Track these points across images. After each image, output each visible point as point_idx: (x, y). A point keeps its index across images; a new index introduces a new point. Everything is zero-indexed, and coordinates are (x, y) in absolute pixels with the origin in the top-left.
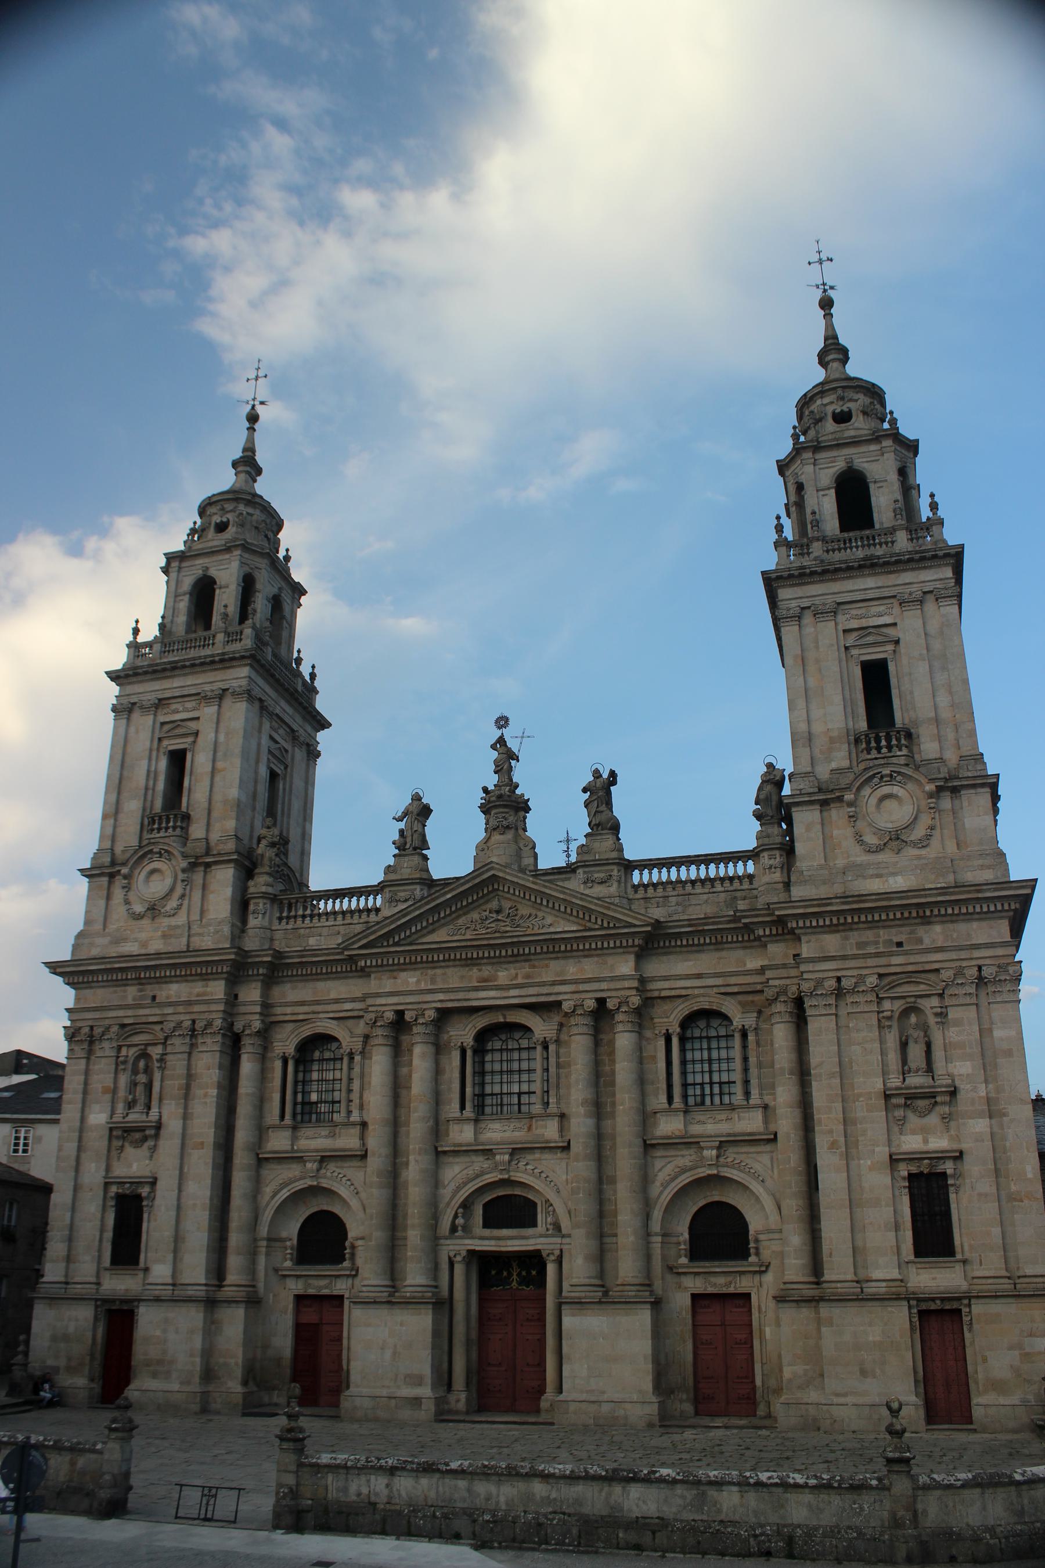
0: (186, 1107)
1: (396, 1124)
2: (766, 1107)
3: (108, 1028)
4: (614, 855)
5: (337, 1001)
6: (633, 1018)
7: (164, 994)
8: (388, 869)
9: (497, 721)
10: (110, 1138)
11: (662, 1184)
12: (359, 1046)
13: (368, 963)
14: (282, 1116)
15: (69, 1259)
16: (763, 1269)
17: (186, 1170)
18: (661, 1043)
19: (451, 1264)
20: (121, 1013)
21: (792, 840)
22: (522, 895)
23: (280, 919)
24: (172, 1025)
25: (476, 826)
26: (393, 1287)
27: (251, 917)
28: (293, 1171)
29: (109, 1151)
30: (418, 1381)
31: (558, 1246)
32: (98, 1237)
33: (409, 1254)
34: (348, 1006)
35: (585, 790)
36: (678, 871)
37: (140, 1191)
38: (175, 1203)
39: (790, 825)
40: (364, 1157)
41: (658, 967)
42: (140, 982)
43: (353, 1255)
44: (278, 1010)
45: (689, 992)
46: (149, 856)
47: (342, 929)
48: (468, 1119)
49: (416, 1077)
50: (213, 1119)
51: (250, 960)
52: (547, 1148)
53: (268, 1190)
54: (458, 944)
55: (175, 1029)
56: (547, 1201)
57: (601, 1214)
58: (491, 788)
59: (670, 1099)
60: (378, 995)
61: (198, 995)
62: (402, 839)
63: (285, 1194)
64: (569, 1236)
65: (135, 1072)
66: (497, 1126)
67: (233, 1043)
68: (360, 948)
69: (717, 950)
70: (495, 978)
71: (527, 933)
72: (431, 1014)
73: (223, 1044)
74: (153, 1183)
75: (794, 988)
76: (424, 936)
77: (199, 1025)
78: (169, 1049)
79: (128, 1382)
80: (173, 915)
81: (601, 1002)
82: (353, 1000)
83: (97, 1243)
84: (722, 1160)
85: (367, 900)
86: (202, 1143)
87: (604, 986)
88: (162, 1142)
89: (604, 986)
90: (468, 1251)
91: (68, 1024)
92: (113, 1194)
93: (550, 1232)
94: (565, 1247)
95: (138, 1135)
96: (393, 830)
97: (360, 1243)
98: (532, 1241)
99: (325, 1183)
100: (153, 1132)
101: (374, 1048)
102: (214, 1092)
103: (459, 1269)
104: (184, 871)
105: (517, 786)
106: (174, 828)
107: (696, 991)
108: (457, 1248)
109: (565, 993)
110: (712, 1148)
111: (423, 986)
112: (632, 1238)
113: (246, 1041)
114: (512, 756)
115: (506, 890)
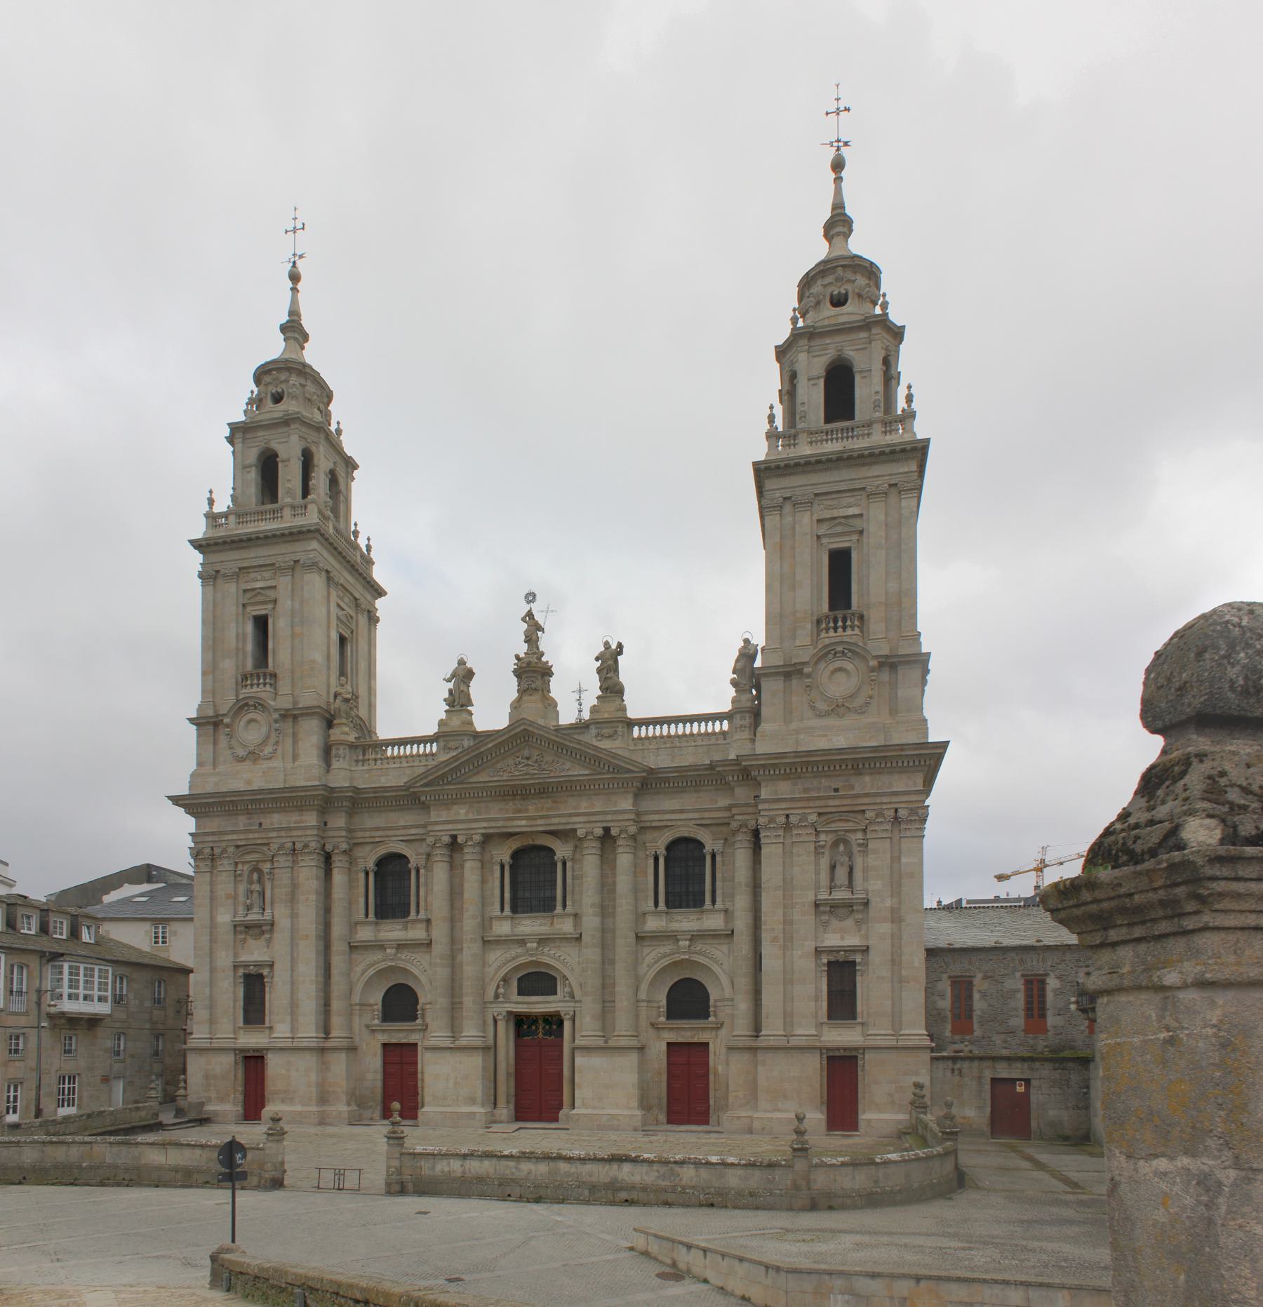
0: (292, 909)
1: (454, 920)
2: (726, 911)
3: (224, 851)
4: (620, 714)
5: (405, 827)
6: (631, 843)
7: (268, 821)
8: (441, 723)
9: (526, 597)
10: (235, 932)
11: (648, 966)
12: (422, 862)
13: (428, 798)
14: (367, 915)
15: (212, 1021)
16: (719, 1026)
17: (295, 956)
18: (651, 861)
19: (495, 1021)
20: (234, 837)
21: (760, 704)
22: (547, 745)
23: (357, 761)
24: (276, 846)
25: (511, 688)
26: (453, 1037)
27: (334, 760)
28: (378, 956)
29: (235, 941)
30: (473, 1101)
31: (572, 1009)
32: (232, 1005)
33: (464, 1014)
34: (413, 831)
35: (597, 659)
36: (669, 728)
37: (261, 971)
38: (290, 979)
39: (759, 691)
40: (429, 944)
41: (649, 804)
42: (249, 813)
43: (423, 1016)
44: (360, 834)
45: (673, 823)
46: (246, 708)
47: (408, 772)
48: (506, 918)
49: (466, 886)
50: (314, 918)
51: (335, 795)
52: (565, 939)
53: (359, 969)
54: (498, 784)
55: (279, 849)
56: (564, 976)
57: (604, 986)
58: (522, 655)
59: (656, 904)
60: (437, 823)
61: (295, 823)
62: (451, 698)
63: (371, 972)
64: (580, 1001)
65: (251, 882)
66: (528, 922)
67: (328, 858)
68: (422, 786)
69: (696, 791)
70: (527, 811)
71: (552, 775)
72: (477, 838)
73: (318, 860)
74: (271, 966)
75: (753, 822)
76: (471, 777)
77: (298, 846)
78: (276, 865)
79: (263, 1106)
80: (271, 758)
81: (607, 830)
82: (417, 827)
83: (232, 1010)
84: (692, 948)
85: (425, 747)
86: (307, 936)
87: (609, 817)
88: (276, 935)
89: (609, 817)
90: (508, 1012)
91: (192, 845)
92: (241, 974)
93: (566, 999)
94: (576, 1009)
95: (256, 931)
96: (444, 689)
97: (428, 1006)
98: (553, 1005)
99: (401, 964)
100: (268, 928)
101: (435, 864)
102: (313, 897)
103: (501, 1025)
104: (276, 721)
105: (542, 654)
106: (265, 684)
107: (679, 823)
108: (500, 1010)
109: (580, 823)
110: (686, 940)
111: (471, 816)
112: (625, 1003)
113: (335, 858)
114: (540, 629)
115: (535, 740)
